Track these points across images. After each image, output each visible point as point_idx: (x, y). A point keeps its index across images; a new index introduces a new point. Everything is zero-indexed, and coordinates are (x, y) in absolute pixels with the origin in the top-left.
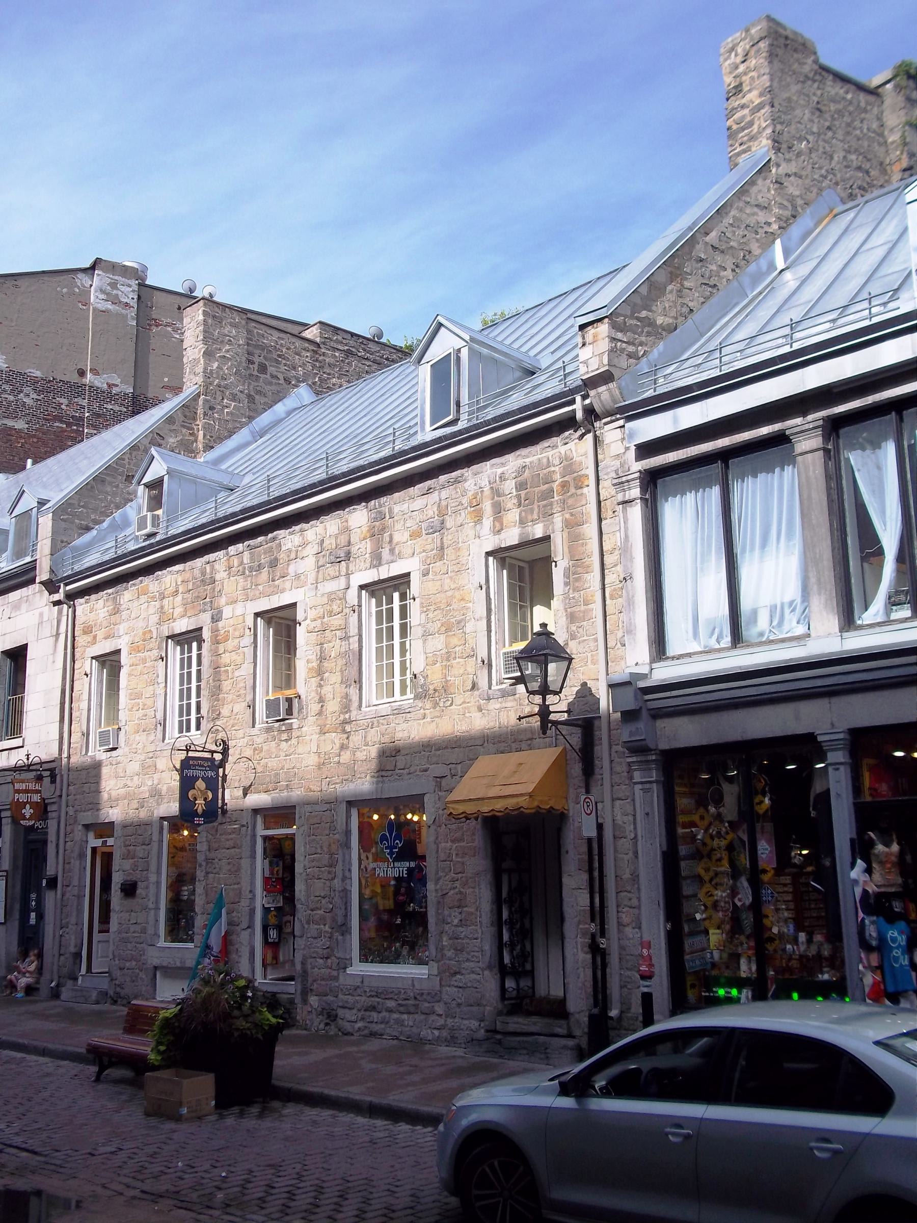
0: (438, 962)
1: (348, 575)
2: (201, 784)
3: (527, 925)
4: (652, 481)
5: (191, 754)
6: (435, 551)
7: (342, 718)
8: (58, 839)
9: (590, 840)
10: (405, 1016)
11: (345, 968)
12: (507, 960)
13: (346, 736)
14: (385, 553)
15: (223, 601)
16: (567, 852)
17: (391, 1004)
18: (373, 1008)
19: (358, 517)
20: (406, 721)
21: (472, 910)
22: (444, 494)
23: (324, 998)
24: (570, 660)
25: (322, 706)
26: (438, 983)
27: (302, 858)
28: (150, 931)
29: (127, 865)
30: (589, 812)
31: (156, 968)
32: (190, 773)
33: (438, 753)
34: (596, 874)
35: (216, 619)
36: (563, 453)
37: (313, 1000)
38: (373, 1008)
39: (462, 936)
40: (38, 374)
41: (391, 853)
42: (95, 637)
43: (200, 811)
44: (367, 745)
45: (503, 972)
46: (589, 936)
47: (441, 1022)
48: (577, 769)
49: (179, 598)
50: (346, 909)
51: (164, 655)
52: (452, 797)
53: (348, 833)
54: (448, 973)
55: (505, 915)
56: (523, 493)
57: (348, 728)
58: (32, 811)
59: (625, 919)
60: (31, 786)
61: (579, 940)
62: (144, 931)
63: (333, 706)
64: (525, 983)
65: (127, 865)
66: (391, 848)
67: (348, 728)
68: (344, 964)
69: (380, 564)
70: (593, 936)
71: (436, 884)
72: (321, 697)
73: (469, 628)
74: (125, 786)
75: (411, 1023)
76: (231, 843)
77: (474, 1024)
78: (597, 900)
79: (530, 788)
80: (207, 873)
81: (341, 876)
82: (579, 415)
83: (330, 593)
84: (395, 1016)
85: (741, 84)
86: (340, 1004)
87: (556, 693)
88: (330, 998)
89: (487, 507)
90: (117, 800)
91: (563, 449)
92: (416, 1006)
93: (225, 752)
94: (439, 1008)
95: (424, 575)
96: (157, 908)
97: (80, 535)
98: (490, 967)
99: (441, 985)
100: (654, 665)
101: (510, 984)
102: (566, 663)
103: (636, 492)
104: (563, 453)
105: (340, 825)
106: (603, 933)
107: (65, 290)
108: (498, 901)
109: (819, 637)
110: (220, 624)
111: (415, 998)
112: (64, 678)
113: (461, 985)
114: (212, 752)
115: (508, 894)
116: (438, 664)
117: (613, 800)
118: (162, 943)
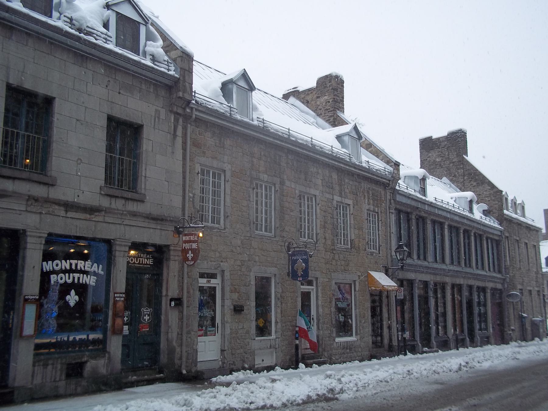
14: (343, 193)
18: (344, 353)
29: (235, 296)
37: (326, 354)
38: (344, 353)
43: (300, 275)
54: (362, 338)
62: (248, 332)
63: (329, 242)
73: (364, 230)
74: (232, 251)
84: (349, 355)
89: (366, 194)
94: (360, 350)
110: (285, 188)
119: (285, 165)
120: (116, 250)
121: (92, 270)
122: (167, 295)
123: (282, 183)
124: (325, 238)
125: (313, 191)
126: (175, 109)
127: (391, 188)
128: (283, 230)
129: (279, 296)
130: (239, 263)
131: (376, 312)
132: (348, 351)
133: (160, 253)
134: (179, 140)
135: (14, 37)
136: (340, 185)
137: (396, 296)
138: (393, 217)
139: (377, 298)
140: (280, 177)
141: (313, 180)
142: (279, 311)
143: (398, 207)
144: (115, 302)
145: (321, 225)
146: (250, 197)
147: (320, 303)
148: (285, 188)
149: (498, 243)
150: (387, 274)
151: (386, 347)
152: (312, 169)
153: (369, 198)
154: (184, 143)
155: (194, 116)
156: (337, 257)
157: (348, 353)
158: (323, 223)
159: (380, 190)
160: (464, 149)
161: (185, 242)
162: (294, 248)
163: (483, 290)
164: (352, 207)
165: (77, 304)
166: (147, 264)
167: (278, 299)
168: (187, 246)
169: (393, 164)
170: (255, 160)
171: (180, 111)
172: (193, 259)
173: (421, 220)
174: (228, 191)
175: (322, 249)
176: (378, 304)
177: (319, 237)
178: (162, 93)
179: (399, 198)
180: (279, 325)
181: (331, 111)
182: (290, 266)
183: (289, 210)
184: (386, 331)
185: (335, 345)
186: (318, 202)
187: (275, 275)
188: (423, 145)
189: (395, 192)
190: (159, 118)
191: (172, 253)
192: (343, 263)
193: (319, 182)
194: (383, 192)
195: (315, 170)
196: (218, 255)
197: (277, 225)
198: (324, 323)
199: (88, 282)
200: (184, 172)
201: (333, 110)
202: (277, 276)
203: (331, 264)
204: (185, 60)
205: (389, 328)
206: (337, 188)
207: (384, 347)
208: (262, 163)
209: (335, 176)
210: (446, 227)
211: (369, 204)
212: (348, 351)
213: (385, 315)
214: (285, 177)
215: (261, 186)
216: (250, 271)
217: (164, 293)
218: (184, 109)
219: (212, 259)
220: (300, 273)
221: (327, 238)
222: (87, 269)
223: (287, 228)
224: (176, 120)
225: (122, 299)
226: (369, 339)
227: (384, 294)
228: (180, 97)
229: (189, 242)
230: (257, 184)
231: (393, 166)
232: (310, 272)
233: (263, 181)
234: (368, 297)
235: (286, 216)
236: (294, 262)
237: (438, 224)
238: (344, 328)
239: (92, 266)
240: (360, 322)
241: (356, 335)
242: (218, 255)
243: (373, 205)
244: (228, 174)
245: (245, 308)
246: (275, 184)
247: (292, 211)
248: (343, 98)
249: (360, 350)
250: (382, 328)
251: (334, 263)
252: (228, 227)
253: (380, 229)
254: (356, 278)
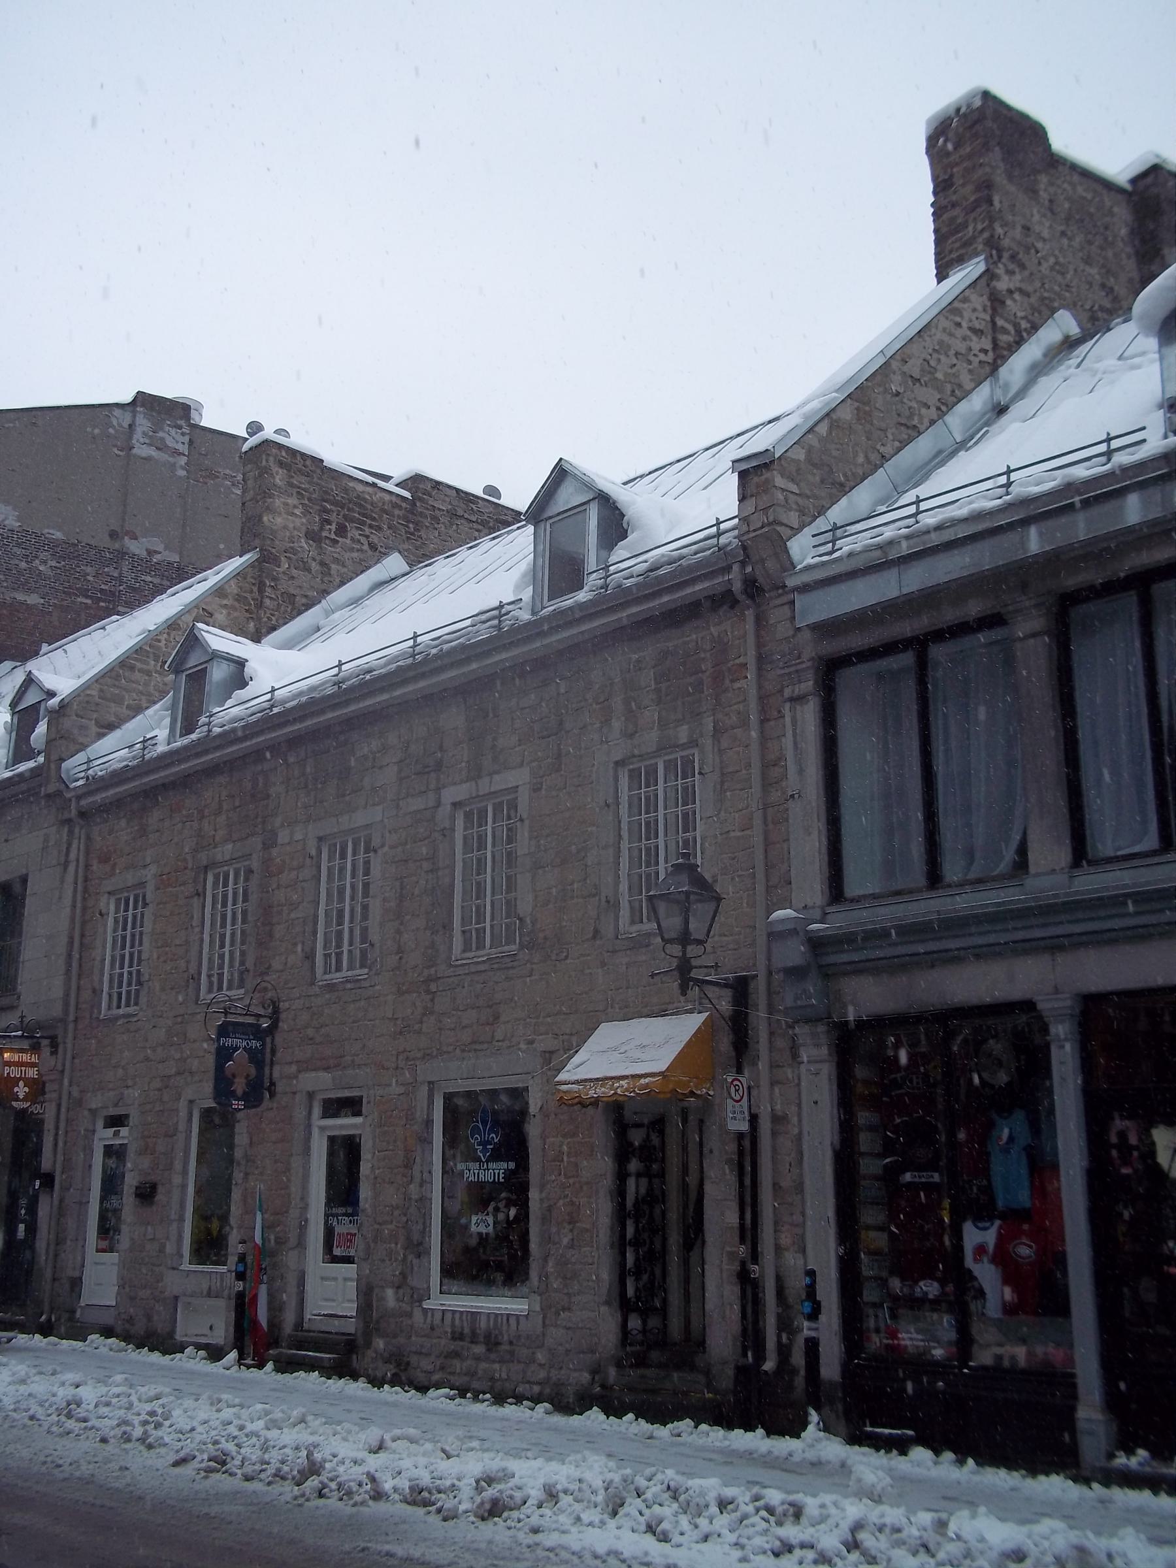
0: (540, 1295)
1: (438, 790)
3: (658, 1246)
4: (830, 670)
5: (231, 1019)
6: (549, 760)
7: (426, 972)
8: (57, 1128)
9: (740, 1136)
10: (497, 1366)
11: (420, 1301)
12: (630, 1292)
13: (429, 997)
15: (278, 821)
16: (711, 1151)
18: (456, 1354)
19: (454, 719)
20: (508, 979)
21: (588, 1226)
23: (394, 1341)
24: (718, 899)
25: (401, 958)
26: (540, 1322)
27: (369, 1156)
28: (170, 1248)
29: (146, 1162)
30: (738, 1098)
31: (176, 1298)
32: (229, 1042)
33: (549, 1019)
34: (748, 1182)
35: (268, 846)
36: (716, 634)
39: (573, 1260)
40: (58, 535)
41: (484, 1151)
43: (239, 1092)
44: (457, 1010)
45: (626, 1306)
46: (737, 1263)
47: (542, 1374)
48: (725, 1043)
49: (222, 819)
50: (424, 1223)
51: (200, 890)
52: (562, 1077)
53: (429, 1123)
55: (630, 1231)
56: (663, 686)
57: (433, 987)
58: (27, 1089)
59: (785, 1239)
60: (25, 1057)
61: (725, 1267)
64: (654, 1322)
65: (146, 1162)
66: (484, 1144)
67: (433, 987)
69: (480, 777)
70: (743, 1264)
71: (541, 1191)
72: (399, 946)
74: (147, 1059)
75: (504, 1376)
78: (748, 1216)
79: (662, 1066)
80: (247, 1174)
81: (417, 1179)
82: (737, 587)
85: (952, 176)
86: (414, 1349)
87: (700, 942)
88: (401, 1340)
89: (617, 702)
91: (714, 630)
92: (512, 1353)
93: (275, 1017)
94: (540, 1356)
95: (535, 790)
96: (182, 1219)
97: (101, 736)
98: (607, 1303)
99: (544, 1325)
100: (829, 910)
101: (635, 1322)
102: (713, 905)
103: (808, 685)
104: (716, 634)
105: (421, 1115)
106: (755, 1256)
107: (97, 431)
108: (621, 1214)
109: (1038, 875)
110: (274, 852)
111: (511, 1343)
112: (73, 920)
113: (570, 1325)
114: (258, 1016)
115: (634, 1205)
116: (551, 906)
117: (773, 1083)
118: (186, 1266)
124: (400, 951)
130: (157, 1084)
132: (479, 1349)
161: (33, 1065)
195: (375, 744)
203: (419, 1032)
212: (479, 1349)
219: (111, 1086)
220: (239, 1086)
233: (226, 863)
238: (492, 1261)
242: (120, 1071)
245: (160, 1189)
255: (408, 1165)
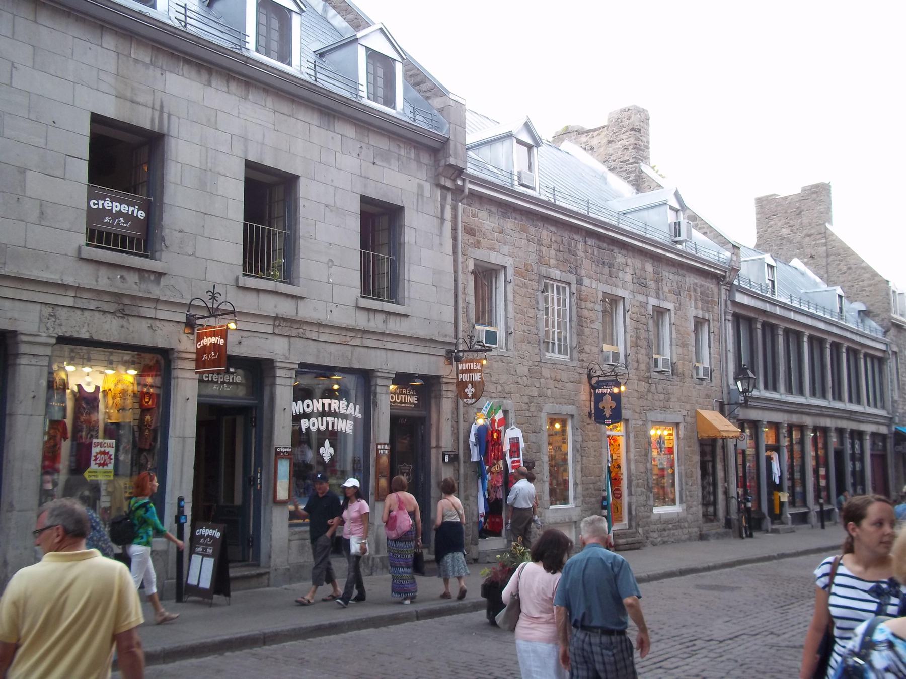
2: (608, 398)
17: (670, 526)
18: (664, 530)
22: (680, 278)
37: (640, 530)
42: (479, 242)
54: (689, 507)
58: (473, 390)
63: (643, 367)
68: (651, 511)
74: (518, 383)
76: (595, 438)
77: (696, 529)
83: (641, 302)
88: (647, 528)
89: (692, 293)
90: (510, 393)
94: (686, 525)
110: (583, 288)
119: (583, 255)
120: (376, 385)
121: (348, 412)
122: (438, 447)
123: (580, 282)
124: (638, 362)
125: (620, 292)
126: (443, 182)
127: (728, 283)
128: (582, 351)
129: (578, 446)
130: (526, 400)
131: (707, 471)
133: (427, 387)
134: (448, 226)
135: (250, 97)
136: (657, 281)
137: (736, 446)
138: (730, 327)
139: (708, 449)
140: (577, 273)
141: (621, 275)
142: (579, 468)
143: (738, 311)
144: (378, 456)
145: (632, 341)
146: (537, 303)
147: (632, 456)
148: (583, 288)
149: (879, 361)
150: (722, 412)
151: (723, 521)
152: (619, 260)
153: (696, 300)
154: (455, 230)
155: (467, 191)
156: (653, 387)
157: (670, 529)
158: (634, 339)
159: (711, 285)
160: (826, 214)
161: (463, 372)
162: (598, 377)
163: (858, 435)
164: (673, 313)
165: (332, 459)
166: (410, 403)
167: (578, 451)
168: (465, 377)
169: (730, 246)
170: (543, 249)
171: (449, 184)
172: (474, 396)
173: (770, 329)
174: (510, 297)
175: (634, 377)
176: (708, 458)
177: (629, 359)
178: (426, 158)
179: (740, 298)
180: (580, 488)
181: (631, 164)
182: (593, 404)
183: (588, 321)
184: (721, 497)
185: (653, 518)
186: (627, 308)
187: (572, 416)
188: (761, 207)
189: (732, 289)
190: (422, 195)
191: (444, 387)
192: (662, 397)
193: (628, 278)
194: (715, 290)
195: (623, 260)
196: (499, 388)
197: (574, 344)
198: (638, 486)
199: (343, 429)
200: (455, 272)
201: (634, 163)
202: (575, 417)
204: (453, 112)
205: (726, 493)
206: (652, 284)
207: (718, 520)
208: (553, 252)
209: (649, 267)
210: (806, 339)
211: (696, 308)
213: (720, 474)
214: (583, 272)
215: (552, 286)
216: (540, 410)
217: (434, 443)
218: (454, 180)
219: (493, 395)
220: (607, 413)
221: (641, 361)
222: (343, 411)
223: (587, 348)
224: (444, 198)
225: (387, 452)
226: (699, 510)
227: (720, 442)
228: (450, 166)
229: (470, 371)
230: (546, 285)
231: (732, 250)
232: (623, 411)
233: (555, 280)
234: (697, 448)
235: (586, 330)
236: (599, 398)
237: (794, 335)
239: (348, 407)
240: (687, 484)
241: (681, 502)
243: (702, 310)
244: (510, 271)
245: (536, 463)
246: (569, 284)
247: (592, 322)
248: (648, 142)
249: (686, 525)
250: (715, 494)
251: (650, 396)
252: (512, 348)
253: (712, 345)
254: (679, 419)
255: (646, 455)
